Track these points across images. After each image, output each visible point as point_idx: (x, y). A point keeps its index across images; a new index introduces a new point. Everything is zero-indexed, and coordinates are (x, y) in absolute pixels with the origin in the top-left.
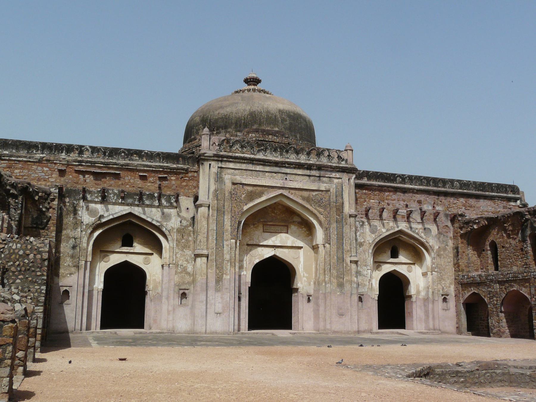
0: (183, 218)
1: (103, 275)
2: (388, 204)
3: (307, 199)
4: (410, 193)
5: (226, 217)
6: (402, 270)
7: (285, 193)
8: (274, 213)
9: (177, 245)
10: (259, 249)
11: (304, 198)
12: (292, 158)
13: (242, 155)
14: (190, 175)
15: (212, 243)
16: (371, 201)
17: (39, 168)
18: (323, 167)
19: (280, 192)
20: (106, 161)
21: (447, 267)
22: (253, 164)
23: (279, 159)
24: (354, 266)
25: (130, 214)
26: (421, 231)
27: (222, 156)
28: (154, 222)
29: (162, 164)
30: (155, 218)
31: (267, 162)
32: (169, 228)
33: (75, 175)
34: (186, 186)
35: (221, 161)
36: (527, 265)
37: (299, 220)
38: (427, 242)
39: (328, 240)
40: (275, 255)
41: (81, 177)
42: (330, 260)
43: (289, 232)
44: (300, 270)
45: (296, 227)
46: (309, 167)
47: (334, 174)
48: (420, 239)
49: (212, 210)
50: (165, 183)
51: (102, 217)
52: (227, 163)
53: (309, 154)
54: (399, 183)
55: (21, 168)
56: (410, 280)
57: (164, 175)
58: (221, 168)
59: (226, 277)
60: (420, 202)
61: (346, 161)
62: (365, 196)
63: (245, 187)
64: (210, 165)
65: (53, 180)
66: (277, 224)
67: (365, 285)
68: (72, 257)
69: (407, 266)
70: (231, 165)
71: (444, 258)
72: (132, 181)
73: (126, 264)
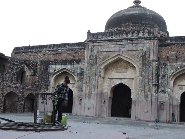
0: (81, 69)
3: (131, 56)
7: (121, 53)
9: (79, 80)
10: (114, 80)
11: (129, 55)
12: (124, 36)
15: (88, 79)
17: (38, 55)
18: (139, 39)
20: (57, 49)
23: (118, 38)
24: (154, 88)
25: (64, 68)
27: (93, 41)
29: (75, 48)
31: (112, 41)
32: (77, 73)
33: (48, 56)
35: (93, 43)
39: (141, 75)
41: (50, 56)
44: (133, 89)
46: (132, 40)
49: (89, 64)
50: (77, 55)
51: (55, 70)
52: (95, 43)
53: (133, 34)
55: (34, 55)
57: (76, 51)
58: (93, 46)
59: (93, 92)
64: (89, 45)
66: (122, 68)
67: (166, 97)
68: (45, 85)
70: (97, 44)
72: (65, 56)
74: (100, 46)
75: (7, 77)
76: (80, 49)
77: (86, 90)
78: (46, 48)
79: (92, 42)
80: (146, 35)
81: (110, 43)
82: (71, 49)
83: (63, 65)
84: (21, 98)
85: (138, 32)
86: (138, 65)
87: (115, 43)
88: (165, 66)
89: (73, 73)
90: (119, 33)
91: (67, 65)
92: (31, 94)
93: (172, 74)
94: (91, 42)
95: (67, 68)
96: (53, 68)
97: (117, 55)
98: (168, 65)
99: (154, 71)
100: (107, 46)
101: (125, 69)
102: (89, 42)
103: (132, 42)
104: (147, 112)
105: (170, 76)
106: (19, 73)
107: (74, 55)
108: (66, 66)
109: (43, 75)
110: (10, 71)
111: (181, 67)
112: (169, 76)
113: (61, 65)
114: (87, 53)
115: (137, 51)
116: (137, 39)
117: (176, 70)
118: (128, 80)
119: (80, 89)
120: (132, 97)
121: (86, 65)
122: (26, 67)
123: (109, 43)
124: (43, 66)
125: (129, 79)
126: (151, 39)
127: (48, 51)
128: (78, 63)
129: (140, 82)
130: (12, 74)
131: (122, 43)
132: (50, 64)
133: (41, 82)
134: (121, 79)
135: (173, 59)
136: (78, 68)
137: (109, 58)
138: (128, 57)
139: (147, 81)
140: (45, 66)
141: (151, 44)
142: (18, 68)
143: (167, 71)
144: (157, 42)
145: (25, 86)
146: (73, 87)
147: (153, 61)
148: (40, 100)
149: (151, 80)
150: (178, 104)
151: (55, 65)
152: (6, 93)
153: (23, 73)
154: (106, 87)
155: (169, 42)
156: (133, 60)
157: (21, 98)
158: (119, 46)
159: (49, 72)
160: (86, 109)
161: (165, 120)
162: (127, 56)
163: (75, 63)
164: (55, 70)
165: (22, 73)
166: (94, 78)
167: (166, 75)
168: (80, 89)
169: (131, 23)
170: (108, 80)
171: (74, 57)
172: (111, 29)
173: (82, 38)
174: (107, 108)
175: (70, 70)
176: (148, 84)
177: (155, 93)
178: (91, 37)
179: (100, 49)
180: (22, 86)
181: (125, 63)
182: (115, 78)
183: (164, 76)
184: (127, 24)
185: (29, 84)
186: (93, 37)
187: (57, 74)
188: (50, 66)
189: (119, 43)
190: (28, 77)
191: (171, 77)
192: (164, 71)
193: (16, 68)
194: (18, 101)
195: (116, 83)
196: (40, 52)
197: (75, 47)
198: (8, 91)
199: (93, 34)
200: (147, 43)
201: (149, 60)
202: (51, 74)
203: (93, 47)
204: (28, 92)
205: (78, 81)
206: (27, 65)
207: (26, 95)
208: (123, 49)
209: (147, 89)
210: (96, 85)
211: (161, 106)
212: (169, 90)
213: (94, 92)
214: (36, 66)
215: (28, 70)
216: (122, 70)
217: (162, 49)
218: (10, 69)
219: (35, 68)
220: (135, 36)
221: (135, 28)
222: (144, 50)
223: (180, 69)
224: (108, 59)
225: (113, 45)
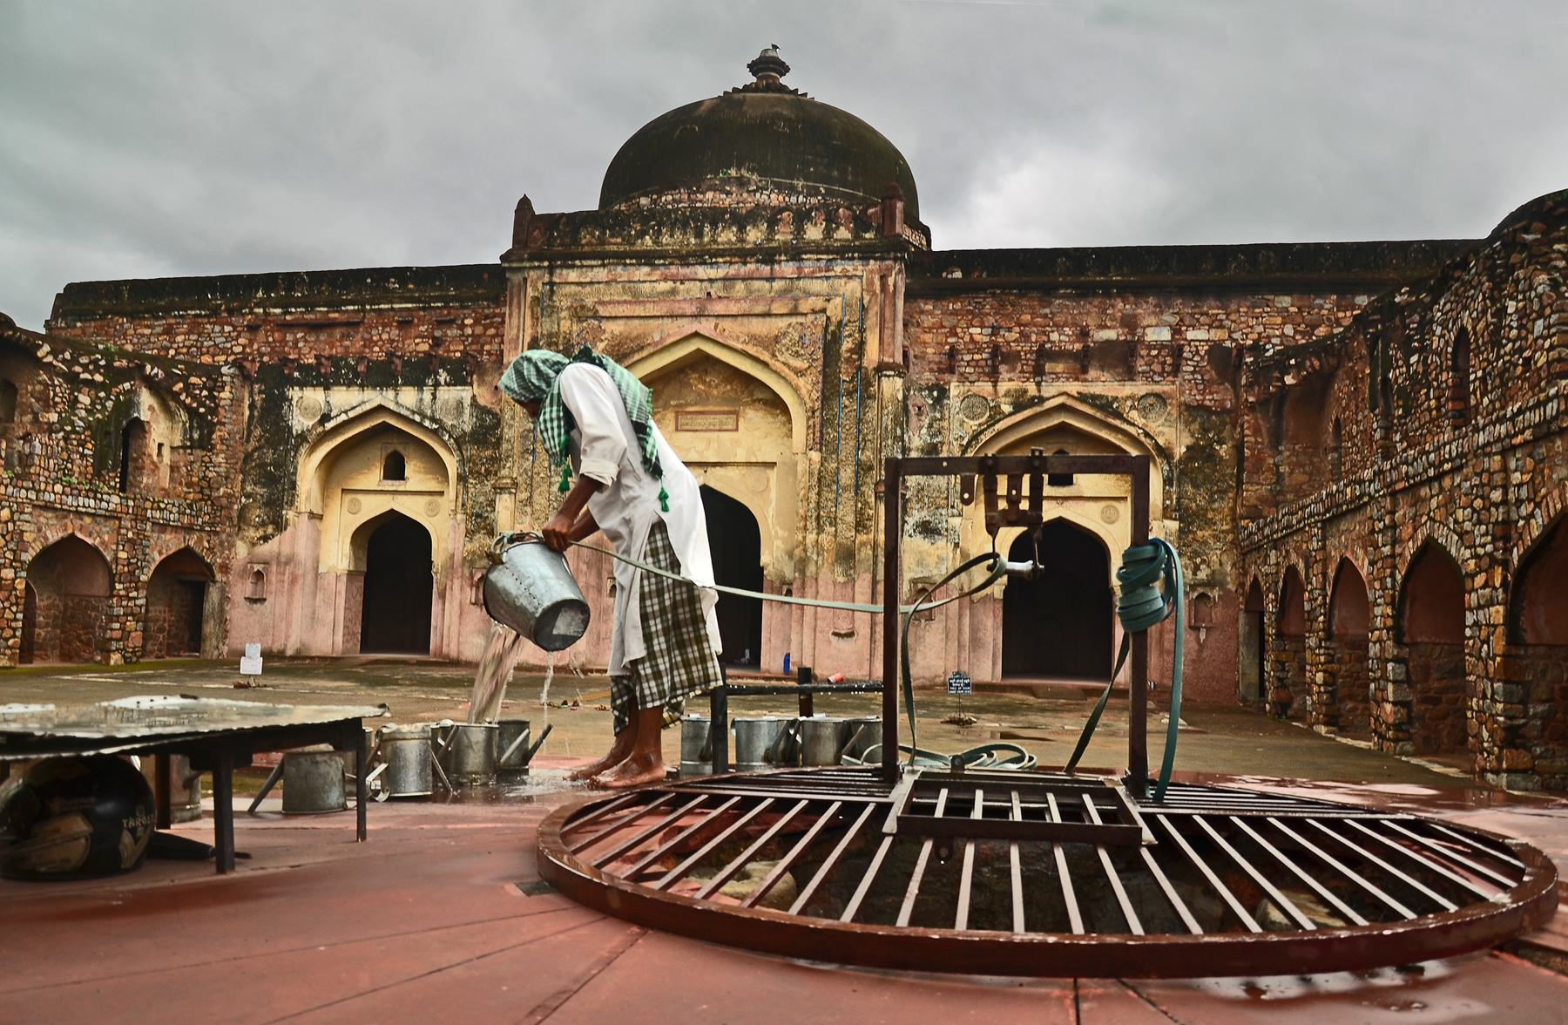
0: (484, 410)
1: (348, 540)
4: (1095, 295)
7: (705, 327)
8: (704, 382)
12: (727, 236)
13: (599, 249)
16: (972, 330)
17: (217, 328)
21: (1216, 505)
22: (625, 265)
25: (380, 409)
26: (1129, 403)
28: (427, 423)
30: (429, 413)
34: (493, 337)
38: (1147, 435)
41: (289, 337)
42: (819, 494)
45: (761, 414)
48: (1125, 426)
50: (453, 332)
51: (326, 418)
52: (565, 272)
53: (773, 223)
55: (189, 332)
62: (953, 320)
63: (606, 325)
65: (240, 349)
67: (941, 559)
69: (1103, 504)
70: (573, 275)
71: (1207, 479)
73: (392, 513)
74: (588, 289)
75: (38, 450)
81: (646, 269)
83: (374, 387)
84: (131, 573)
85: (802, 217)
86: (804, 391)
88: (938, 402)
89: (435, 432)
90: (696, 220)
91: (395, 387)
92: (186, 552)
93: (969, 443)
96: (306, 405)
99: (888, 421)
101: (724, 413)
103: (765, 269)
104: (850, 635)
106: (108, 433)
107: (438, 333)
108: (391, 394)
109: (253, 444)
110: (54, 417)
111: (1018, 407)
113: (362, 386)
115: (794, 320)
116: (796, 253)
118: (744, 470)
119: (480, 522)
120: (765, 559)
122: (146, 399)
124: (251, 395)
125: (749, 464)
127: (278, 311)
128: (458, 380)
129: (814, 481)
130: (65, 439)
132: (294, 383)
133: (243, 482)
135: (977, 364)
136: (460, 403)
137: (645, 353)
139: (847, 476)
140: (260, 392)
142: (104, 406)
143: (945, 424)
144: (900, 271)
145: (148, 505)
146: (433, 511)
147: (881, 368)
148: (241, 589)
151: (327, 388)
152: (38, 547)
153: (138, 428)
155: (958, 275)
156: (778, 366)
157: (131, 573)
159: (290, 429)
161: (941, 672)
162: (739, 346)
163: (443, 376)
164: (326, 418)
167: (942, 443)
168: (480, 522)
169: (752, 170)
171: (437, 343)
172: (644, 201)
173: (489, 244)
175: (417, 418)
180: (131, 503)
181: (727, 381)
184: (733, 172)
185: (167, 494)
186: (544, 238)
188: (295, 393)
189: (702, 272)
190: (159, 454)
192: (930, 426)
194: (112, 596)
197: (440, 288)
198: (46, 538)
199: (552, 220)
200: (850, 278)
202: (302, 437)
203: (552, 292)
204: (172, 543)
205: (462, 478)
206: (161, 391)
207: (158, 559)
209: (851, 518)
214: (210, 390)
215: (161, 416)
216: (711, 419)
217: (922, 312)
218: (48, 405)
219: (204, 405)
221: (776, 199)
223: (1011, 414)
224: (637, 357)
225: (665, 280)
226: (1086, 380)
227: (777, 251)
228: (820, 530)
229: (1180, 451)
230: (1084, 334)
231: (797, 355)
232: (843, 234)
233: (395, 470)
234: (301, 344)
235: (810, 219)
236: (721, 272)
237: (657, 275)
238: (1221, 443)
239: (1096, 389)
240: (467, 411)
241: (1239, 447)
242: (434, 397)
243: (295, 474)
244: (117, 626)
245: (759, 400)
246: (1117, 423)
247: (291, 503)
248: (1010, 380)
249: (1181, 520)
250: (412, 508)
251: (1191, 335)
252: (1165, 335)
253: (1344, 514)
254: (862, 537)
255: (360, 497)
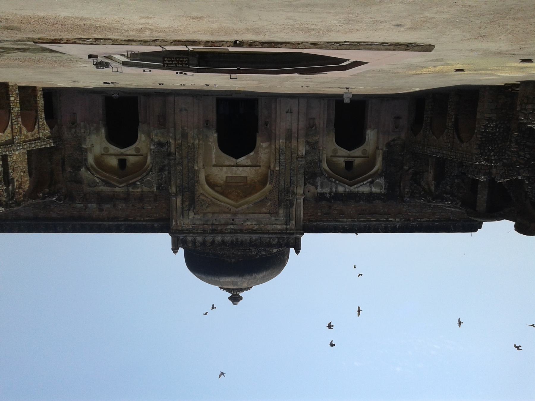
1: (367, 140)
2: (133, 206)
5: (283, 187)
6: (113, 149)
13: (270, 236)
14: (307, 217)
17: (414, 214)
18: (201, 233)
19: (237, 210)
20: (368, 223)
21: (71, 152)
27: (286, 233)
35: (287, 229)
36: (10, 156)
37: (216, 188)
38: (93, 174)
39: (196, 173)
40: (237, 158)
42: (194, 156)
43: (225, 178)
46: (214, 231)
47: (191, 227)
51: (371, 183)
53: (213, 241)
54: (123, 225)
56: (105, 139)
58: (286, 225)
60: (101, 210)
61: (178, 240)
65: (405, 207)
67: (156, 135)
70: (279, 227)
73: (350, 150)
74: (274, 223)
76: (316, 221)
77: (298, 144)
78: (395, 227)
79: (288, 231)
80: (190, 238)
81: (254, 229)
82: (337, 221)
85: (204, 243)
87: (245, 228)
93: (149, 172)
94: (292, 232)
95: (345, 187)
97: (240, 206)
98: (155, 188)
99: (173, 179)
100: (259, 223)
102: (295, 231)
105: (151, 169)
108: (347, 190)
110: (456, 181)
111: (134, 183)
112: (153, 170)
113: (358, 193)
114: (299, 213)
115: (205, 211)
116: (204, 232)
117: (142, 179)
119: (313, 146)
120: (216, 135)
121: (300, 191)
123: (256, 227)
125: (222, 166)
126: (182, 230)
127: (390, 219)
131: (232, 227)
132: (384, 195)
134: (237, 165)
136: (322, 187)
138: (219, 203)
139: (185, 162)
141: (180, 222)
146: (335, 151)
147: (176, 195)
149: (178, 164)
150: (140, 124)
154: (264, 152)
155: (155, 225)
158: (237, 221)
159: (385, 179)
160: (295, 109)
164: (371, 183)
165: (439, 177)
166: (282, 167)
168: (313, 146)
170: (261, 164)
171: (330, 207)
174: (262, 113)
175: (337, 182)
176: (182, 158)
177: (170, 142)
178: (292, 241)
179: (273, 218)
182: (249, 168)
183: (161, 170)
184: (233, 260)
187: (367, 175)
188: (383, 191)
189: (236, 227)
191: (149, 168)
192: (162, 178)
193: (448, 187)
195: (247, 158)
196: (409, 220)
197: (330, 225)
201: (183, 196)
202: (380, 176)
203: (286, 222)
205: (321, 161)
208: (229, 216)
209: (183, 148)
210: (277, 154)
211: (162, 122)
212: (152, 147)
213: (282, 141)
220: (209, 238)
222: (192, 215)
223: (137, 181)
226: (114, 192)
227: (210, 233)
228: (193, 144)
229: (83, 169)
230: (114, 206)
231: (203, 200)
232: (190, 238)
233: (349, 165)
234: (381, 208)
235: (201, 243)
236: (229, 227)
237: (251, 227)
238: (70, 171)
239: (109, 189)
240: (319, 184)
241: (64, 170)
242: (331, 189)
243: (383, 163)
244: (430, 107)
245: (219, 186)
246: (103, 178)
247: (384, 153)
248: (137, 192)
249: (81, 148)
250: (343, 152)
251: (82, 205)
252: (89, 205)
253: (3, 145)
254: (180, 142)
255: (362, 155)
